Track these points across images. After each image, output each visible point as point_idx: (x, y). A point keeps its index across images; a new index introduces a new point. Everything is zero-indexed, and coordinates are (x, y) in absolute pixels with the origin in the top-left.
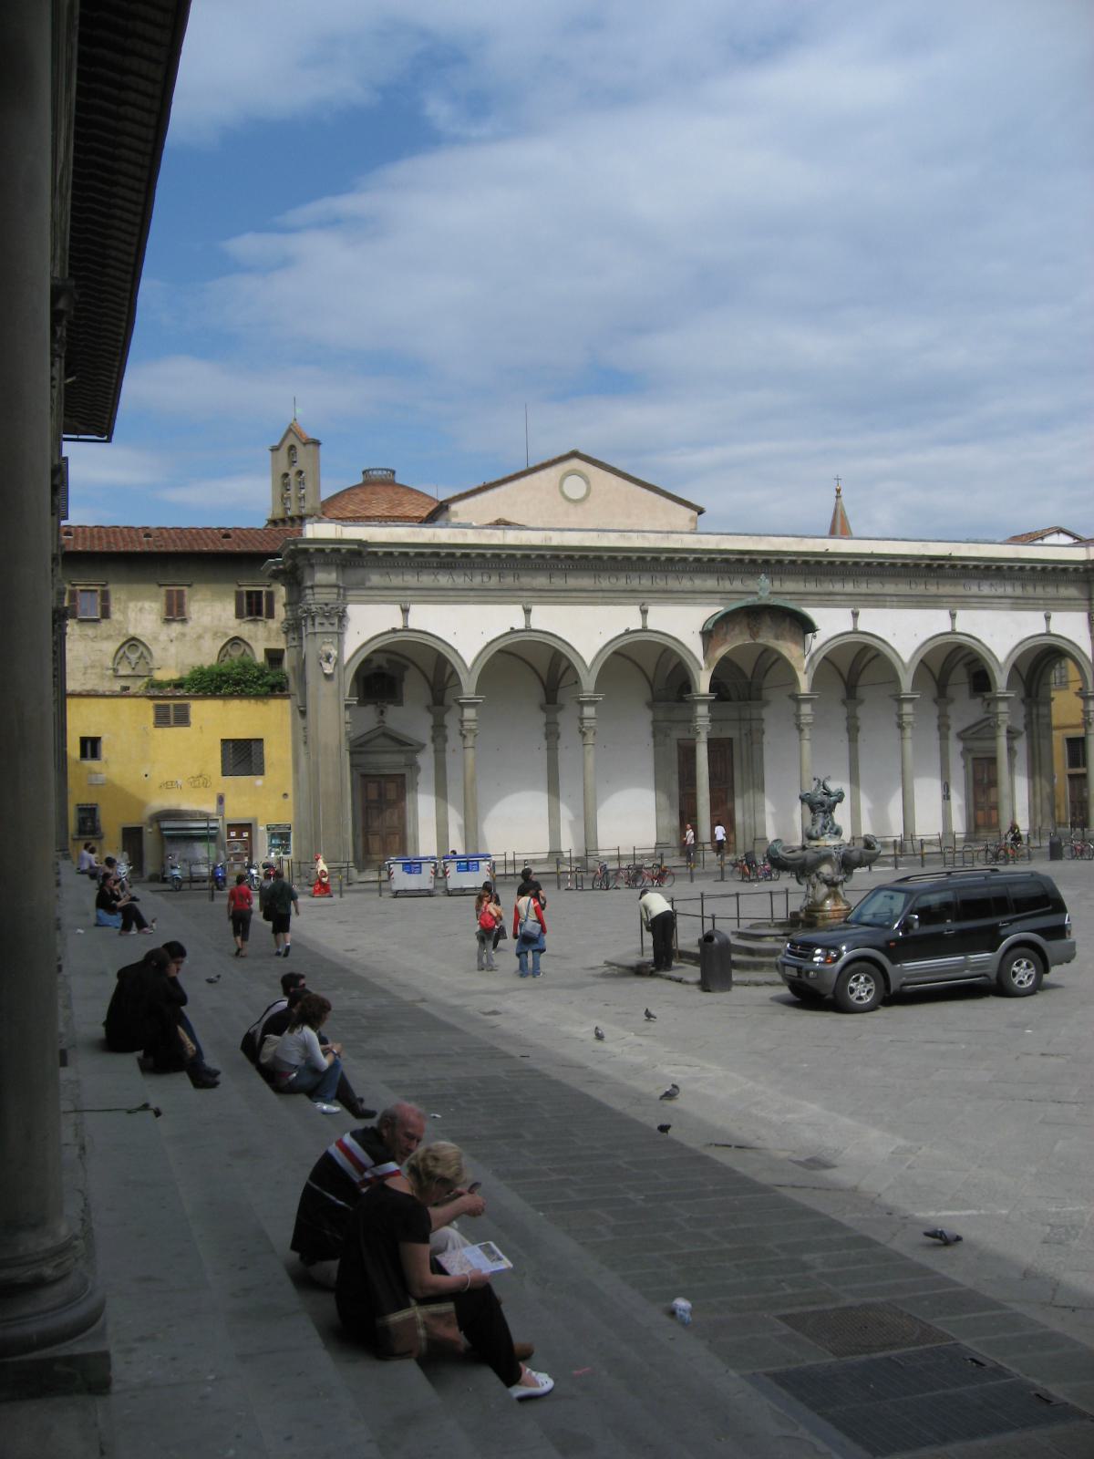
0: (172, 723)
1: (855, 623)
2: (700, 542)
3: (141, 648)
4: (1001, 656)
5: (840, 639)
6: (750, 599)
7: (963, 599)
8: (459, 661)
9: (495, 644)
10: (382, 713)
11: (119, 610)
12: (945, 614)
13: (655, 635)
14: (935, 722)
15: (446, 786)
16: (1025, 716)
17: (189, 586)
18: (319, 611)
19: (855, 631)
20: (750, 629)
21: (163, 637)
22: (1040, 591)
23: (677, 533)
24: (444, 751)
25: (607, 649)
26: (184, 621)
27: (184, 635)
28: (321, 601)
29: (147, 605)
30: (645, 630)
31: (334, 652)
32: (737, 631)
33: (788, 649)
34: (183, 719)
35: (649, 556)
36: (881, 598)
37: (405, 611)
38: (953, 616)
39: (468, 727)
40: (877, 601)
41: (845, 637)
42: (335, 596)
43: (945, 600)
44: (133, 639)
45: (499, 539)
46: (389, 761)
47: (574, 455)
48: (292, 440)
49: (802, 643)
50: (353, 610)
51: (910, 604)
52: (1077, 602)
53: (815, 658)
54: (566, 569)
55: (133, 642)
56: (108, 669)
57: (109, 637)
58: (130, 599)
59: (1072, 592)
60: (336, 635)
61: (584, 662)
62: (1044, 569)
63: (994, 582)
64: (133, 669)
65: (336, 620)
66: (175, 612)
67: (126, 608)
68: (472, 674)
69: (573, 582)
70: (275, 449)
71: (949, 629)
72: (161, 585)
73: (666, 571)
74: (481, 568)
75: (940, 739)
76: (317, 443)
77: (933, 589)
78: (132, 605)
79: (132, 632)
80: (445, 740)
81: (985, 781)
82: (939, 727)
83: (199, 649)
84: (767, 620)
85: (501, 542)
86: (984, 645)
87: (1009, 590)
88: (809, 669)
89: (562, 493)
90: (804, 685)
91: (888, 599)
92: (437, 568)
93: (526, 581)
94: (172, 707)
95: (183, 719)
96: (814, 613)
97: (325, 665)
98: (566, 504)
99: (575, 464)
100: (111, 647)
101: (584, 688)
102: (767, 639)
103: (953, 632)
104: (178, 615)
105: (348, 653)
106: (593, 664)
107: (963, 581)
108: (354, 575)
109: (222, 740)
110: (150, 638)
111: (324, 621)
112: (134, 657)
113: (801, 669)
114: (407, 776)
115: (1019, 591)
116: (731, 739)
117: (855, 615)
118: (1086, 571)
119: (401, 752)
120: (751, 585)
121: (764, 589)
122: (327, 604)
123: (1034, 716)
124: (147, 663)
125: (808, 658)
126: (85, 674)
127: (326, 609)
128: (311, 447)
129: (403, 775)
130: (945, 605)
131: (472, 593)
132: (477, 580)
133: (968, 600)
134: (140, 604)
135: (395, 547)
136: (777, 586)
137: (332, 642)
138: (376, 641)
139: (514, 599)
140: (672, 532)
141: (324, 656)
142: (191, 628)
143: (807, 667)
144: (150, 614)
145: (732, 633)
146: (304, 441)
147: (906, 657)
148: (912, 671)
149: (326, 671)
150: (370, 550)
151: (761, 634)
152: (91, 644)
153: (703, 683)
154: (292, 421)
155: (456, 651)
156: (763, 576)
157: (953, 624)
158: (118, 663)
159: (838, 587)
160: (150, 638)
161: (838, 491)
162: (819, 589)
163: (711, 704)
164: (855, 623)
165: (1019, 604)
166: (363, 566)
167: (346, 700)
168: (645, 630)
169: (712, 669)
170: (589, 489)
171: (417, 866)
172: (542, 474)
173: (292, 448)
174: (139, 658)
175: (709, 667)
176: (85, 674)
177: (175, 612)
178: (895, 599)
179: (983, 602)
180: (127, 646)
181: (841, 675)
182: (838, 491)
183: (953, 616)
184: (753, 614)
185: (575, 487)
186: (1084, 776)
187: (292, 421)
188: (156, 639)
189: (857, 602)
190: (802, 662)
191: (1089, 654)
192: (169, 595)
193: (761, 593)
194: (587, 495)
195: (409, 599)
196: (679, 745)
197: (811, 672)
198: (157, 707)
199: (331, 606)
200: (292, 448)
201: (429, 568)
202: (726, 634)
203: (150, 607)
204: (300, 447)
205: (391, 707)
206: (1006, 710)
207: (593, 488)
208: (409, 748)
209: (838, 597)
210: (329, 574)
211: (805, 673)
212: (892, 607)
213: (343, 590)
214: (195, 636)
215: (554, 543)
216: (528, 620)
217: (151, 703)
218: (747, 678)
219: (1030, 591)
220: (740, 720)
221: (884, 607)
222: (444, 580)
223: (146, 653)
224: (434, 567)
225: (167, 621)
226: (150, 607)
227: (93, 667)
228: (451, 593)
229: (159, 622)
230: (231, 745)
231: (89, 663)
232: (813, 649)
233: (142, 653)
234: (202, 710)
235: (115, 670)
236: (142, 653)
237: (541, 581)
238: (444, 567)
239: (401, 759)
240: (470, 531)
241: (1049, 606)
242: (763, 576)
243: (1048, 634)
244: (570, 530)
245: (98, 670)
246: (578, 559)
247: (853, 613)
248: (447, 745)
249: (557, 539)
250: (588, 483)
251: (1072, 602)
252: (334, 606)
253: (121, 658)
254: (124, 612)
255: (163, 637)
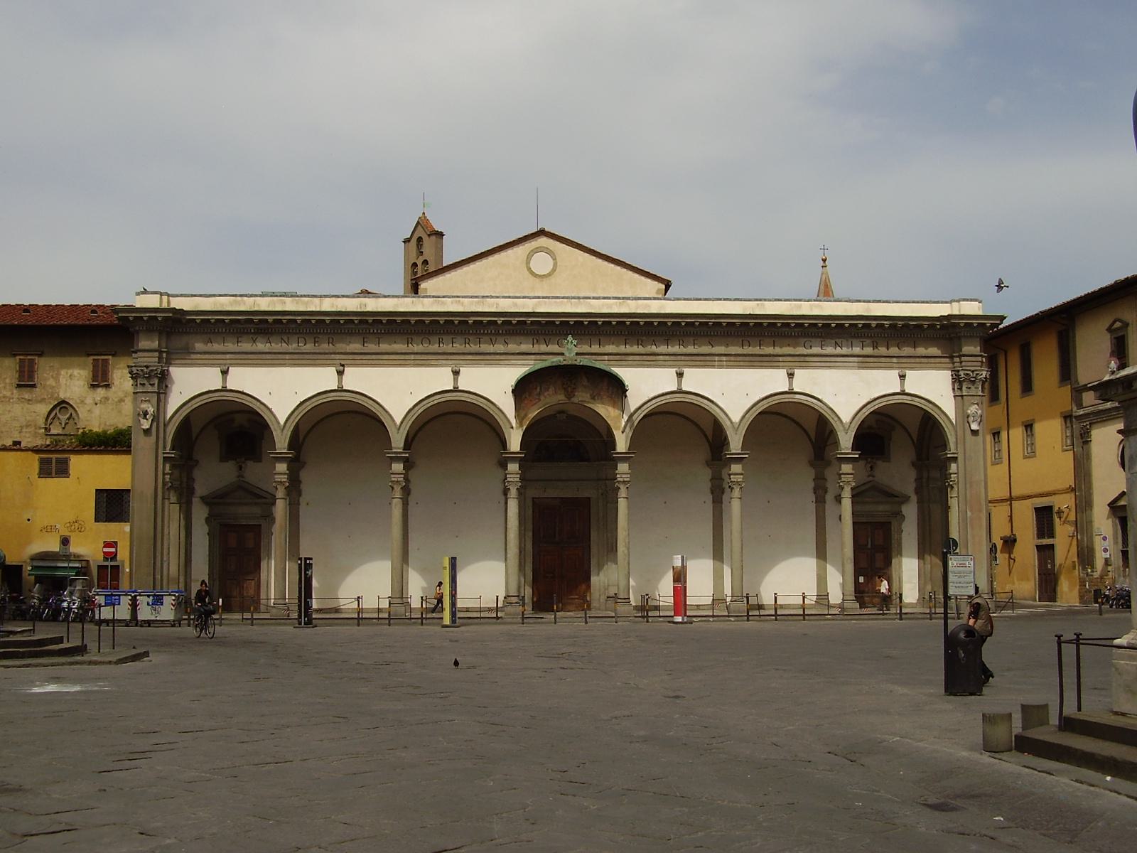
0: (54, 475)
1: (680, 383)
2: (515, 305)
3: (71, 410)
4: (846, 416)
5: (662, 398)
6: (555, 360)
7: (802, 359)
8: (273, 419)
9: (308, 403)
10: (240, 468)
11: (52, 376)
12: (782, 373)
13: (467, 395)
14: (812, 485)
15: (298, 536)
16: (916, 480)
17: (113, 355)
18: (141, 373)
19: (680, 391)
20: (565, 389)
21: (89, 401)
22: (894, 351)
23: (492, 297)
24: (299, 504)
25: (417, 408)
26: (108, 386)
27: (107, 399)
28: (142, 364)
29: (76, 372)
30: (456, 390)
31: (151, 410)
32: (551, 390)
33: (606, 411)
34: (63, 470)
35: (456, 320)
36: (708, 358)
37: (225, 373)
38: (791, 376)
39: (279, 480)
40: (704, 361)
41: (668, 397)
42: (157, 359)
43: (781, 359)
44: (63, 402)
45: (316, 308)
46: (246, 513)
47: (542, 233)
48: (420, 232)
49: (620, 403)
50: (177, 372)
51: (742, 364)
52: (938, 360)
53: (634, 417)
54: (377, 333)
55: (63, 405)
56: (40, 428)
57: (42, 401)
58: (62, 367)
59: (934, 351)
60: (155, 395)
61: (394, 421)
62: (893, 326)
63: (839, 341)
64: (64, 428)
65: (156, 381)
66: (100, 379)
67: (59, 374)
68: (285, 431)
69: (384, 347)
70: (406, 241)
71: (787, 389)
72: (89, 355)
73: (480, 334)
74: (296, 333)
75: (816, 502)
76: (441, 235)
77: (769, 350)
78: (63, 372)
79: (62, 396)
80: (300, 494)
81: (869, 546)
82: (815, 490)
83: (120, 412)
84: (585, 382)
85: (318, 310)
86: (825, 404)
87: (857, 350)
88: (628, 428)
89: (529, 269)
90: (622, 444)
91: (717, 358)
92: (254, 333)
93: (341, 347)
94: (54, 461)
95: (63, 470)
96: (624, 373)
97: (143, 421)
98: (532, 278)
99: (543, 241)
100: (44, 409)
101: (393, 445)
102: (582, 396)
103: (791, 392)
104: (103, 381)
105: (171, 409)
106: (402, 423)
107: (802, 340)
108: (179, 342)
109: (97, 490)
110: (78, 401)
111: (145, 382)
112: (64, 418)
113: (618, 428)
114: (263, 525)
115: (868, 350)
116: (589, 498)
117: (680, 375)
118: (943, 326)
119: (256, 504)
120: (554, 348)
121: (570, 351)
122: (147, 367)
123: (924, 480)
124: (75, 423)
125: (626, 418)
126: (20, 432)
127: (145, 370)
128: (433, 238)
129: (260, 525)
130: (781, 364)
131: (287, 356)
132: (293, 347)
133: (807, 359)
134: (70, 372)
135: (212, 315)
136: (586, 348)
137: (149, 401)
138: (197, 400)
139: (329, 362)
140: (487, 297)
141: (141, 413)
142: (113, 393)
143: (625, 427)
144: (78, 380)
145: (546, 394)
146: (429, 233)
147: (736, 418)
148: (743, 431)
149: (144, 427)
150: (188, 318)
151: (576, 394)
152: (27, 406)
153: (515, 442)
154: (421, 215)
155: (270, 410)
156: (570, 338)
157: (791, 384)
158: (50, 424)
159: (663, 349)
160: (78, 401)
161: (824, 260)
162: (641, 349)
163: (523, 463)
164: (680, 383)
165: (866, 362)
166: (186, 333)
167: (164, 453)
168: (456, 390)
169: (524, 428)
170: (555, 265)
171: (117, 597)
172: (510, 252)
173: (420, 239)
174: (69, 419)
175: (521, 425)
176: (20, 432)
177: (100, 379)
178: (724, 358)
179: (826, 361)
180: (59, 408)
181: (706, 436)
182: (824, 260)
183: (791, 376)
184: (568, 375)
185: (542, 263)
186: (1051, 547)
187: (421, 215)
188: (82, 402)
189: (681, 362)
190: (620, 422)
191: (952, 415)
192: (22, 362)
193: (567, 354)
194: (554, 270)
195: (228, 362)
196: (534, 503)
197: (629, 432)
198: (41, 461)
199: (151, 368)
200: (420, 239)
201: (247, 333)
202: (539, 394)
203: (79, 373)
204: (425, 238)
205: (250, 463)
206: (851, 471)
207: (558, 264)
208: (263, 500)
209: (661, 358)
210: (153, 342)
211: (623, 432)
212: (721, 367)
213: (169, 356)
214: (116, 400)
215: (369, 309)
216: (340, 381)
217: (37, 457)
218: (602, 437)
219: (882, 350)
220: (599, 480)
221: (713, 367)
222: (261, 346)
223: (74, 415)
224: (252, 333)
225: (93, 386)
226: (79, 373)
227: (27, 426)
228: (268, 356)
229: (86, 386)
230: (105, 495)
231: (24, 424)
232: (632, 410)
233: (71, 414)
234: (80, 464)
235: (47, 430)
236: (71, 414)
237: (356, 346)
238: (261, 333)
239: (257, 510)
240: (288, 300)
241: (904, 364)
242: (570, 338)
243: (903, 393)
244: (343, 296)
245: (32, 429)
246: (385, 324)
247: (677, 373)
248: (301, 498)
249: (314, 305)
250: (554, 259)
251: (932, 360)
252: (155, 368)
253: (53, 419)
254: (56, 378)
255: (89, 401)
